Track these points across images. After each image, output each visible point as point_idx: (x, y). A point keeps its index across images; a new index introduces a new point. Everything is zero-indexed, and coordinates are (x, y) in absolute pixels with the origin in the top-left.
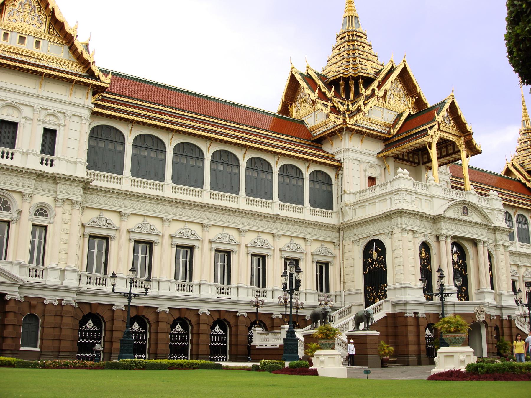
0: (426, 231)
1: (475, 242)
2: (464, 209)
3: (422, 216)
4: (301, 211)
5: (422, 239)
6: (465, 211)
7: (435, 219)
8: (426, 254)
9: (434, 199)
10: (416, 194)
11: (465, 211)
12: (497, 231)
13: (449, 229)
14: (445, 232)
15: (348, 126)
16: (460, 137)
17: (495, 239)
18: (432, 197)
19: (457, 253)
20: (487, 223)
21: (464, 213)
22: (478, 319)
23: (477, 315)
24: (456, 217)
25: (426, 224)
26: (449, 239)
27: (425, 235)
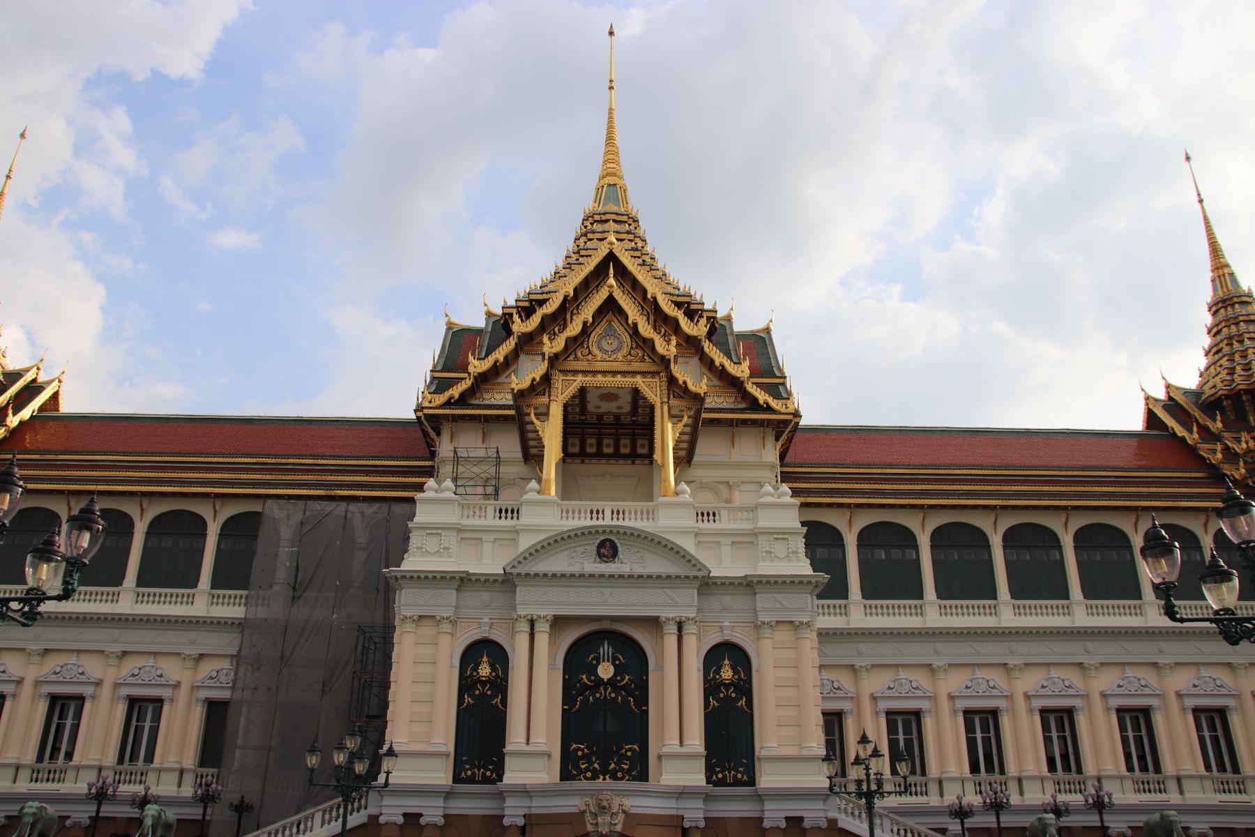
1: (654, 623)
2: (602, 545)
3: (464, 581)
6: (607, 550)
7: (507, 582)
8: (493, 669)
9: (521, 535)
10: (459, 531)
11: (607, 550)
12: (758, 588)
14: (522, 611)
15: (426, 411)
16: (658, 373)
18: (517, 532)
19: (615, 659)
20: (695, 573)
21: (599, 554)
23: (588, 818)
24: (576, 568)
25: (485, 596)
26: (543, 628)
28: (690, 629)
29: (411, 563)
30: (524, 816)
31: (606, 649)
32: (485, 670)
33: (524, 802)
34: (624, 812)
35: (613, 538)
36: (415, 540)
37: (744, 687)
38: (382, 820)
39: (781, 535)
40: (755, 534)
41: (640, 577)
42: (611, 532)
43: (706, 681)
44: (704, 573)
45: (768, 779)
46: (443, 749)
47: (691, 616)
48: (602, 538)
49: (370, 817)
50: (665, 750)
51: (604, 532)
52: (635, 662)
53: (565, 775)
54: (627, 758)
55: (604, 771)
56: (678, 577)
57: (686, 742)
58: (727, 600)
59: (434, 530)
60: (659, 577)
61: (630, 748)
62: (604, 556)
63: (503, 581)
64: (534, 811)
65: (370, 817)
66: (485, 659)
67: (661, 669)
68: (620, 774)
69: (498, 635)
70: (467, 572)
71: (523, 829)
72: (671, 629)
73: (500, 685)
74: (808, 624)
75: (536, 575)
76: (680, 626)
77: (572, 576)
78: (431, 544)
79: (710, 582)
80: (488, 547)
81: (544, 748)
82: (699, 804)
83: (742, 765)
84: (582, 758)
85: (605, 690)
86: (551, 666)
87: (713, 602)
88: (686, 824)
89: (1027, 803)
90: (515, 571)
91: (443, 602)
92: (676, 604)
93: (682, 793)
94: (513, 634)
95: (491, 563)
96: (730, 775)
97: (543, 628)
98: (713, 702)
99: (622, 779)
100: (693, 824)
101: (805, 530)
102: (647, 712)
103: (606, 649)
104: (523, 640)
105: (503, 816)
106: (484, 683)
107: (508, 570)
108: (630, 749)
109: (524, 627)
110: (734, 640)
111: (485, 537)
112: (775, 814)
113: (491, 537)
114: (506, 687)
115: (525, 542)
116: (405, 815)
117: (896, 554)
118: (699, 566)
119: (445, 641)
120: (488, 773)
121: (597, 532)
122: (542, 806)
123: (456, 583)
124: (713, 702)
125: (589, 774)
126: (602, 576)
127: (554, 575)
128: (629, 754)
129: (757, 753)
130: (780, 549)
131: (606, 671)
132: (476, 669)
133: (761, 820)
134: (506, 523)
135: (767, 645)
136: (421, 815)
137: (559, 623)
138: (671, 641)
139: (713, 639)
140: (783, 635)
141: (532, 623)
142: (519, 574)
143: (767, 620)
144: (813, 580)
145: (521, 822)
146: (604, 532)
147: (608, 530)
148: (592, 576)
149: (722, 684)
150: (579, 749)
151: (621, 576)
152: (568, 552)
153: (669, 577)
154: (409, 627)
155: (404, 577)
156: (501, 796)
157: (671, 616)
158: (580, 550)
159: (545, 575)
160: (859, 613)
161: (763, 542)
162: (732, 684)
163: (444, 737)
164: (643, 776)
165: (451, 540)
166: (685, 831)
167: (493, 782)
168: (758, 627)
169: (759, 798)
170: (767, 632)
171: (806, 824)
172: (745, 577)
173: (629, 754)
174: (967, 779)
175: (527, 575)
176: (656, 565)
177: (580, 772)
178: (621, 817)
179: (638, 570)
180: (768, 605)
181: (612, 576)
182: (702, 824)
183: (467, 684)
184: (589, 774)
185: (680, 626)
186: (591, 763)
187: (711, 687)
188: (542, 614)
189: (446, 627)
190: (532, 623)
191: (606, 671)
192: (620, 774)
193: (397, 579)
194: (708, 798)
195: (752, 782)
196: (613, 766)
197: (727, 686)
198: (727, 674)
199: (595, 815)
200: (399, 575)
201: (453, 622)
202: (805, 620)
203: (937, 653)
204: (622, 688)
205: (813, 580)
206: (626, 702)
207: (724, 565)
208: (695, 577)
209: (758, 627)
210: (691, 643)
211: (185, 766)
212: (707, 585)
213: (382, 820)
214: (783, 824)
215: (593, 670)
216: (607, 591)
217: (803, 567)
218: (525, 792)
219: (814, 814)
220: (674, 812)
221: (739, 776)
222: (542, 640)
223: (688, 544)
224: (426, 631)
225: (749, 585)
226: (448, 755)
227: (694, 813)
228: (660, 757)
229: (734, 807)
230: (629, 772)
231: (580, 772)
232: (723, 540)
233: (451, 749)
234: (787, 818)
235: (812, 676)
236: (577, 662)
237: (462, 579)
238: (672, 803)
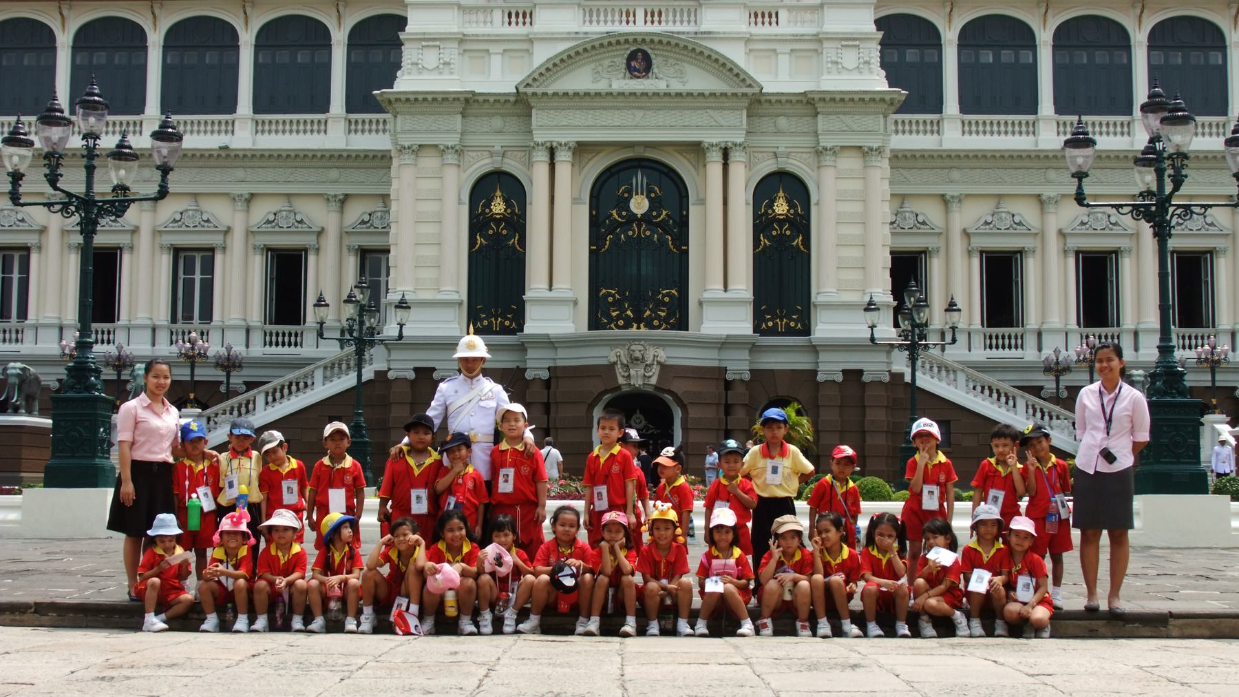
0: (497, 143)
1: (696, 150)
2: (632, 57)
3: (469, 103)
4: (323, 127)
5: (481, 165)
7: (520, 105)
8: (508, 204)
9: (536, 45)
11: (639, 60)
13: (557, 127)
14: (540, 137)
17: (816, 134)
18: (531, 41)
19: (649, 191)
21: (629, 68)
22: (621, 381)
23: (619, 371)
24: (602, 86)
25: (497, 122)
27: (492, 154)
28: (737, 157)
29: (405, 83)
30: (549, 369)
31: (639, 179)
32: (498, 207)
33: (548, 354)
34: (659, 363)
35: (645, 48)
36: (409, 54)
37: (801, 224)
38: (391, 375)
39: (850, 41)
40: (818, 39)
41: (679, 95)
42: (644, 40)
43: (756, 216)
44: (756, 90)
45: (824, 328)
46: (455, 297)
47: (740, 140)
48: (633, 48)
49: (377, 373)
50: (706, 295)
51: (635, 40)
52: (673, 194)
53: (594, 324)
54: (665, 304)
55: (638, 320)
56: (724, 95)
57: (730, 287)
58: (782, 122)
59: (430, 40)
60: (702, 95)
61: (668, 293)
62: (635, 70)
63: (516, 102)
64: (560, 363)
65: (377, 373)
66: (498, 193)
67: (702, 202)
68: (656, 323)
69: (512, 166)
70: (473, 93)
71: (547, 383)
72: (715, 158)
73: (517, 223)
74: (879, 151)
75: (555, 94)
76: (726, 153)
77: (598, 94)
78: (430, 58)
79: (763, 99)
80: (496, 61)
81: (570, 295)
82: (745, 355)
83: (796, 312)
84: (613, 304)
85: (639, 227)
86: (576, 201)
87: (766, 124)
88: (729, 377)
89: (1141, 359)
90: (530, 91)
91: (448, 130)
92: (725, 128)
93: (726, 343)
94: (530, 164)
95: (499, 78)
96: (781, 324)
97: (563, 157)
98: (764, 241)
99: (658, 327)
100: (738, 377)
101: (880, 35)
102: (687, 251)
103: (639, 179)
104: (540, 172)
105: (525, 369)
106: (498, 222)
107: (522, 90)
108: (668, 295)
109: (542, 157)
110: (790, 168)
111: (493, 48)
112: (830, 368)
113: (499, 48)
114: (524, 225)
115: (542, 55)
116: (416, 370)
117: (1007, 56)
118: (748, 82)
119: (451, 174)
120: (507, 323)
121: (627, 41)
122: (567, 358)
123: (459, 107)
124: (764, 241)
125: (621, 323)
126: (633, 94)
127: (576, 94)
128: (667, 299)
129: (813, 299)
130: (850, 58)
131: (639, 205)
132: (488, 205)
133: (815, 372)
134: (518, 30)
135: (828, 176)
136: (434, 369)
137: (582, 150)
138: (714, 170)
139: (767, 167)
140: (850, 163)
141: (552, 152)
142: (534, 94)
143: (829, 145)
144: (887, 97)
145: (545, 375)
146: (635, 40)
147: (639, 38)
148: (621, 94)
149: (775, 219)
150: (610, 295)
151: (656, 94)
152: (593, 66)
153: (713, 95)
154: (408, 159)
155: (397, 100)
156: (522, 348)
157: (714, 141)
158: (607, 62)
159: (566, 94)
160: (954, 132)
161: (830, 51)
162: (787, 219)
163: (456, 285)
164: (683, 324)
165: (451, 52)
166: (728, 385)
167: (512, 332)
168: (819, 152)
169: (814, 349)
170: (828, 160)
171: (866, 378)
172: (805, 94)
173: (667, 299)
174: (1073, 331)
175: (545, 94)
176: (698, 80)
177: (611, 319)
178: (656, 370)
179: (676, 86)
180: (831, 130)
181: (644, 94)
182: (747, 377)
183: (478, 223)
184: (621, 323)
185: (726, 153)
186: (623, 311)
187: (762, 223)
188: (563, 141)
189: (451, 158)
190: (552, 152)
191: (639, 205)
192: (656, 323)
193: (390, 102)
194: (754, 348)
195: (807, 331)
196: (648, 313)
197: (781, 223)
198: (781, 208)
199: (626, 367)
200: (392, 98)
201: (459, 151)
202: (875, 146)
203: (1049, 182)
204: (658, 225)
205: (887, 97)
206: (663, 243)
207: (779, 77)
208: (745, 95)
209: (819, 152)
210: (739, 173)
211: (158, 323)
212: (758, 104)
213: (391, 375)
214: (840, 378)
215: (623, 204)
216: (639, 114)
217: (878, 82)
218: (549, 343)
219: (874, 367)
220: (715, 364)
221: (792, 324)
222: (564, 170)
223: (736, 54)
224: (429, 162)
225: (811, 104)
226: (460, 304)
227: (739, 365)
228: (701, 304)
229: (783, 357)
230: (666, 320)
231: (611, 319)
232: (779, 47)
233: (465, 297)
234: (844, 372)
235: (882, 211)
236: (605, 195)
237: (467, 101)
238: (713, 354)
